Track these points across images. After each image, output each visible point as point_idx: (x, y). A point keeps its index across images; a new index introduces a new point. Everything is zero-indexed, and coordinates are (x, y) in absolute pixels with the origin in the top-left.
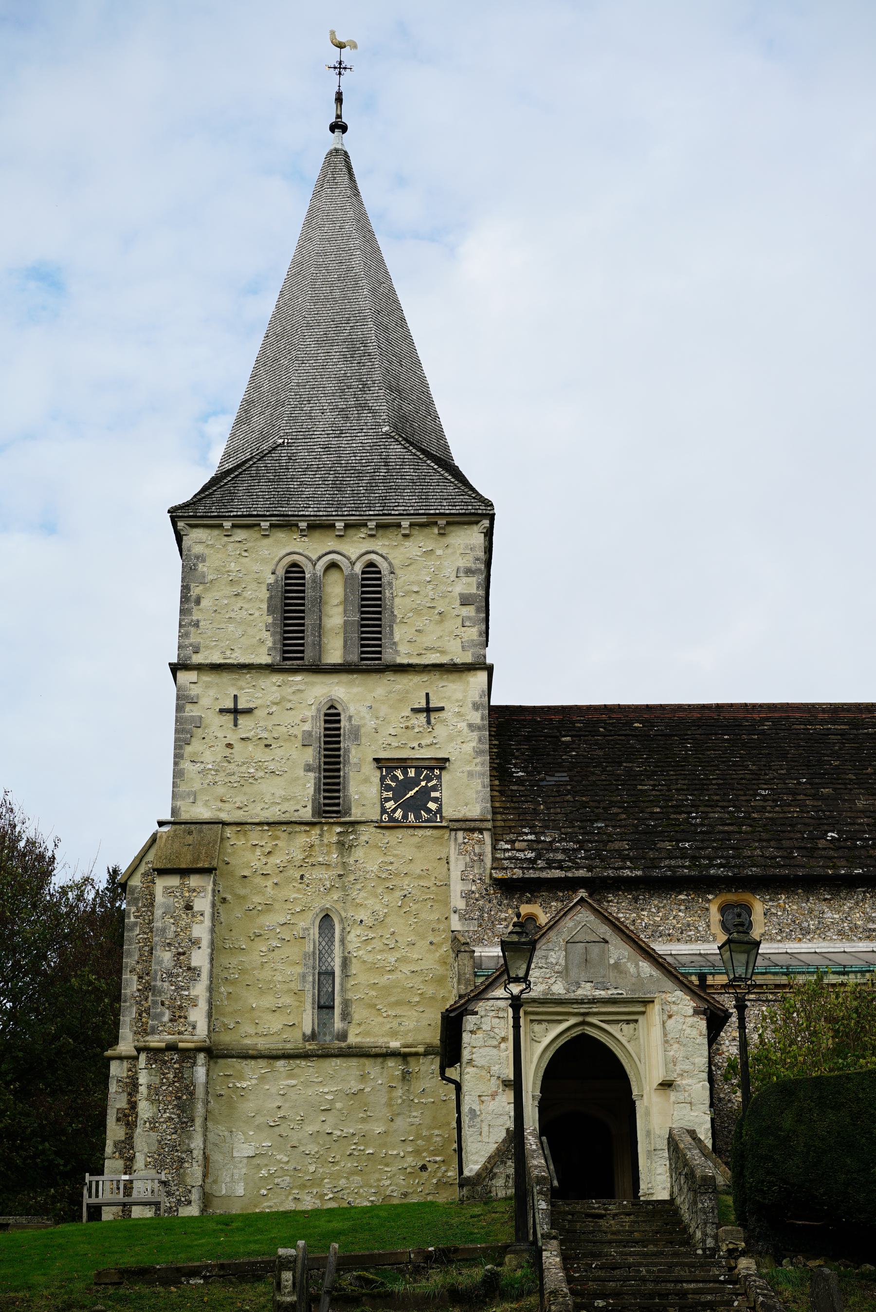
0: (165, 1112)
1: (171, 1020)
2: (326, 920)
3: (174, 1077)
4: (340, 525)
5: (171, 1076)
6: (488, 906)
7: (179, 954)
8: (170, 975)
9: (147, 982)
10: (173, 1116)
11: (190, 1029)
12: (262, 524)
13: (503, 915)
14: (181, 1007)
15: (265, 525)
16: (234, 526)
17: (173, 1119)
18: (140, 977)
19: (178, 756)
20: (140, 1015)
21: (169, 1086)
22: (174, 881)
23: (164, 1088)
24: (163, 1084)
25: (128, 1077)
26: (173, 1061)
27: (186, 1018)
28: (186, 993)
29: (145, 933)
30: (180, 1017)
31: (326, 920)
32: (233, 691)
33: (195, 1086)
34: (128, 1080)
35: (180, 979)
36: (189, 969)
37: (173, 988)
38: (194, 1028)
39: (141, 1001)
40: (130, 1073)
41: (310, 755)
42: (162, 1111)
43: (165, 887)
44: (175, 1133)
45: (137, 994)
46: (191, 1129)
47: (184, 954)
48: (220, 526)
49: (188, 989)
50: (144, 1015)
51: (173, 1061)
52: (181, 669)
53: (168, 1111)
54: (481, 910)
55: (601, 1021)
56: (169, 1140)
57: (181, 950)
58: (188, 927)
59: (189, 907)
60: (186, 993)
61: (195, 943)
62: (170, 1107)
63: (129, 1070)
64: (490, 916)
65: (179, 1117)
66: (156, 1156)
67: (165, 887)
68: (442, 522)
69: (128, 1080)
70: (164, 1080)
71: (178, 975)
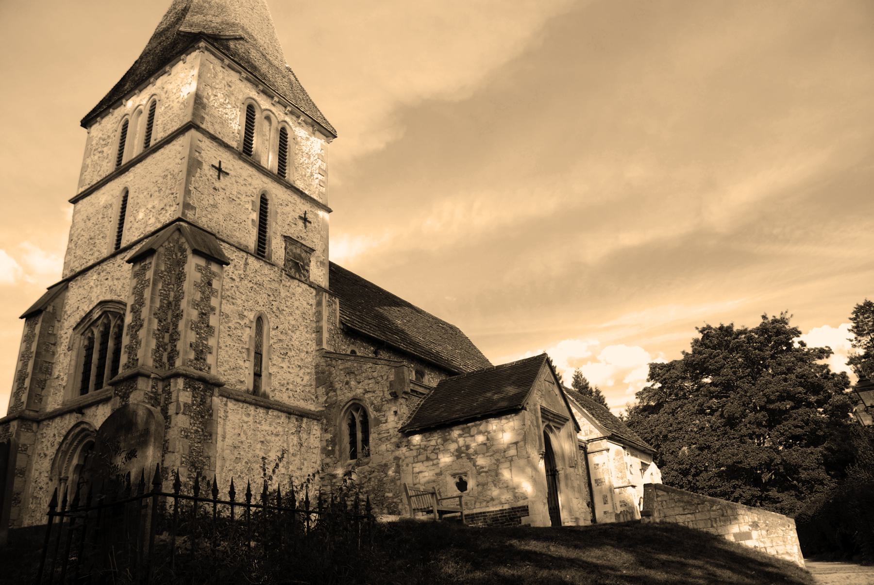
0: (194, 426)
1: (196, 359)
2: (260, 320)
3: (201, 401)
4: (276, 99)
5: (199, 400)
6: (337, 340)
7: (203, 313)
8: (197, 327)
9: (164, 325)
10: (199, 430)
11: (207, 369)
12: (243, 73)
13: (344, 348)
14: (202, 351)
15: (244, 75)
16: (229, 66)
17: (199, 431)
18: (160, 321)
19: (188, 182)
20: (158, 348)
21: (197, 407)
22: (202, 262)
23: (195, 407)
24: (193, 404)
25: (152, 392)
26: (200, 389)
27: (205, 360)
28: (205, 342)
29: (165, 290)
30: (201, 358)
31: (260, 320)
32: (219, 159)
33: (213, 411)
34: (152, 395)
35: (202, 331)
36: (208, 326)
37: (198, 336)
38: (209, 368)
39: (159, 338)
40: (154, 390)
41: (255, 216)
42: (193, 425)
43: (197, 264)
44: (200, 442)
45: (157, 332)
46: (210, 441)
47: (205, 314)
48: (222, 60)
49: (207, 340)
50: (161, 349)
51: (200, 389)
52: (194, 128)
53: (196, 425)
54: (335, 341)
55: (554, 426)
56: (196, 447)
57: (203, 311)
58: (208, 299)
59: (210, 284)
60: (205, 342)
61: (213, 309)
62: (198, 422)
63: (153, 387)
64: (338, 346)
65: (203, 431)
66: (188, 458)
67: (197, 264)
68: (316, 127)
69: (152, 395)
70: (195, 402)
71: (201, 328)
